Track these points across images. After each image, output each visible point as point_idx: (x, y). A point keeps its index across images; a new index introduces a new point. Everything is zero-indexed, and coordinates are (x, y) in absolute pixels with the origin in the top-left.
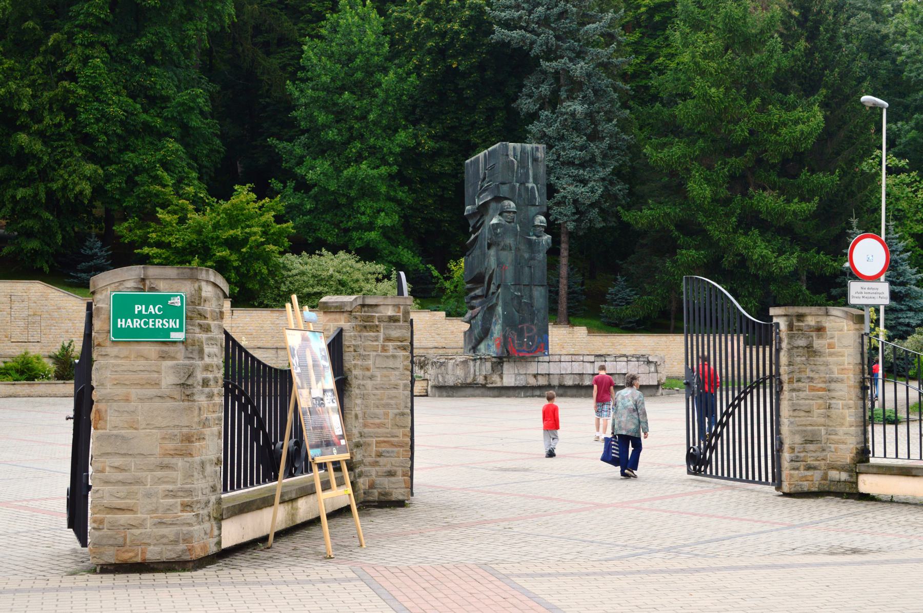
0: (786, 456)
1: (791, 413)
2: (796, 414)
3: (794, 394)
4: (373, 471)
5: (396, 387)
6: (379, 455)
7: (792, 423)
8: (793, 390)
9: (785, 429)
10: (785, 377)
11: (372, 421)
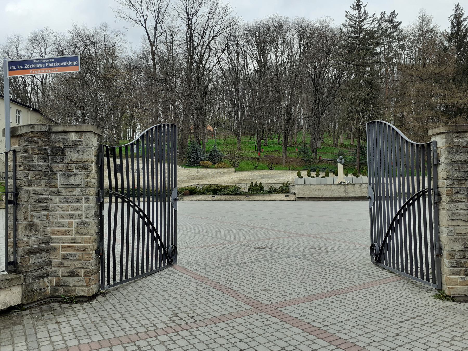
0: (446, 261)
1: (450, 223)
2: (455, 223)
3: (453, 205)
4: (60, 271)
5: (78, 200)
6: (64, 258)
7: (451, 232)
8: (452, 201)
9: (444, 237)
10: (443, 190)
11: (57, 229)
